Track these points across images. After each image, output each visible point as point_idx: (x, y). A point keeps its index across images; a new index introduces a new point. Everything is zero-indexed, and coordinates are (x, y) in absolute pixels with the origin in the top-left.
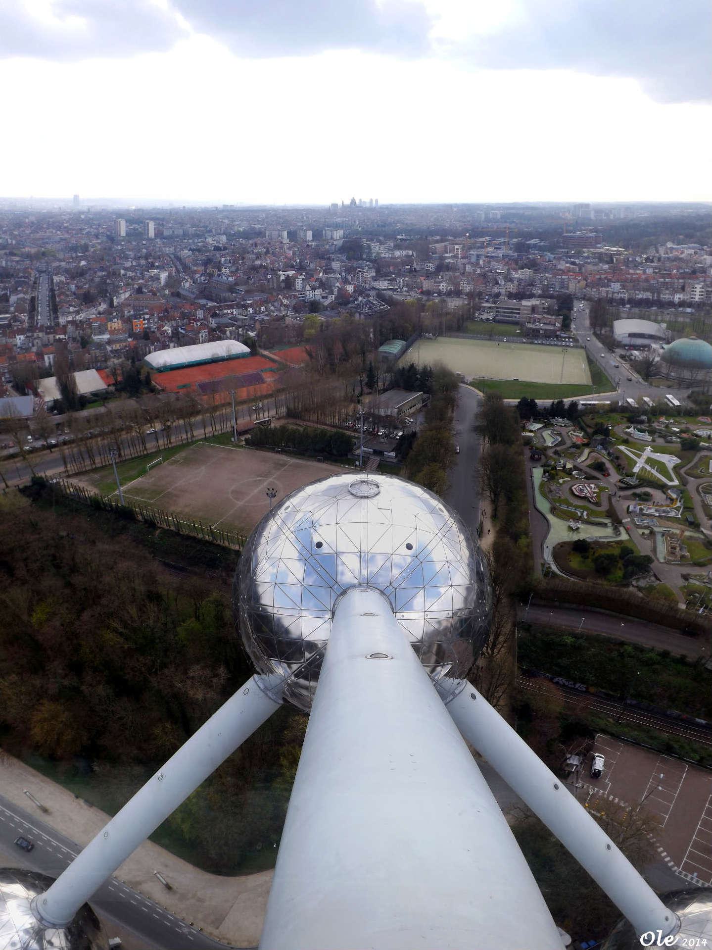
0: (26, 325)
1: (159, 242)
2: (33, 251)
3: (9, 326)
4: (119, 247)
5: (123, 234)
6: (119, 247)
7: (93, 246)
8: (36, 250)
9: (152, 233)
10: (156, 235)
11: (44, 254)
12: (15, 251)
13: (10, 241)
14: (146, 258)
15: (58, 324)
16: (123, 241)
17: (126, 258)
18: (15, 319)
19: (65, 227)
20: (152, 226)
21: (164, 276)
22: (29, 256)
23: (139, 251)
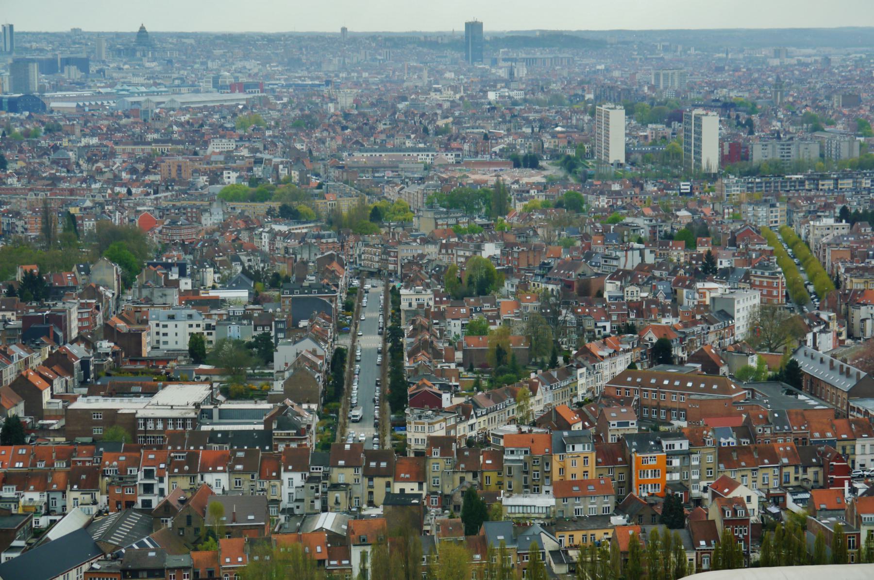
0: (312, 442)
1: (734, 185)
2: (346, 205)
3: (266, 437)
4: (603, 202)
5: (617, 153)
6: (603, 202)
7: (522, 194)
8: (355, 202)
9: (711, 155)
10: (724, 160)
11: (377, 215)
12: (303, 208)
13: (283, 172)
14: (689, 237)
15: (401, 448)
16: (616, 178)
17: (621, 237)
18: (283, 419)
19: (438, 131)
20: (711, 134)
21: (746, 305)
22: (334, 221)
23: (668, 214)
